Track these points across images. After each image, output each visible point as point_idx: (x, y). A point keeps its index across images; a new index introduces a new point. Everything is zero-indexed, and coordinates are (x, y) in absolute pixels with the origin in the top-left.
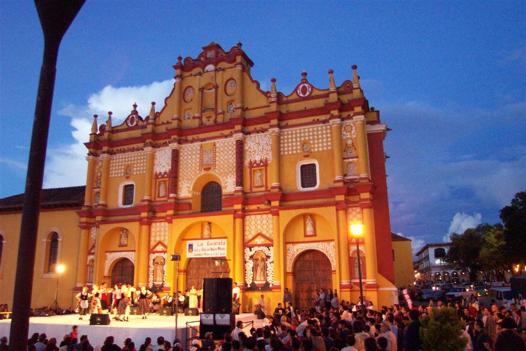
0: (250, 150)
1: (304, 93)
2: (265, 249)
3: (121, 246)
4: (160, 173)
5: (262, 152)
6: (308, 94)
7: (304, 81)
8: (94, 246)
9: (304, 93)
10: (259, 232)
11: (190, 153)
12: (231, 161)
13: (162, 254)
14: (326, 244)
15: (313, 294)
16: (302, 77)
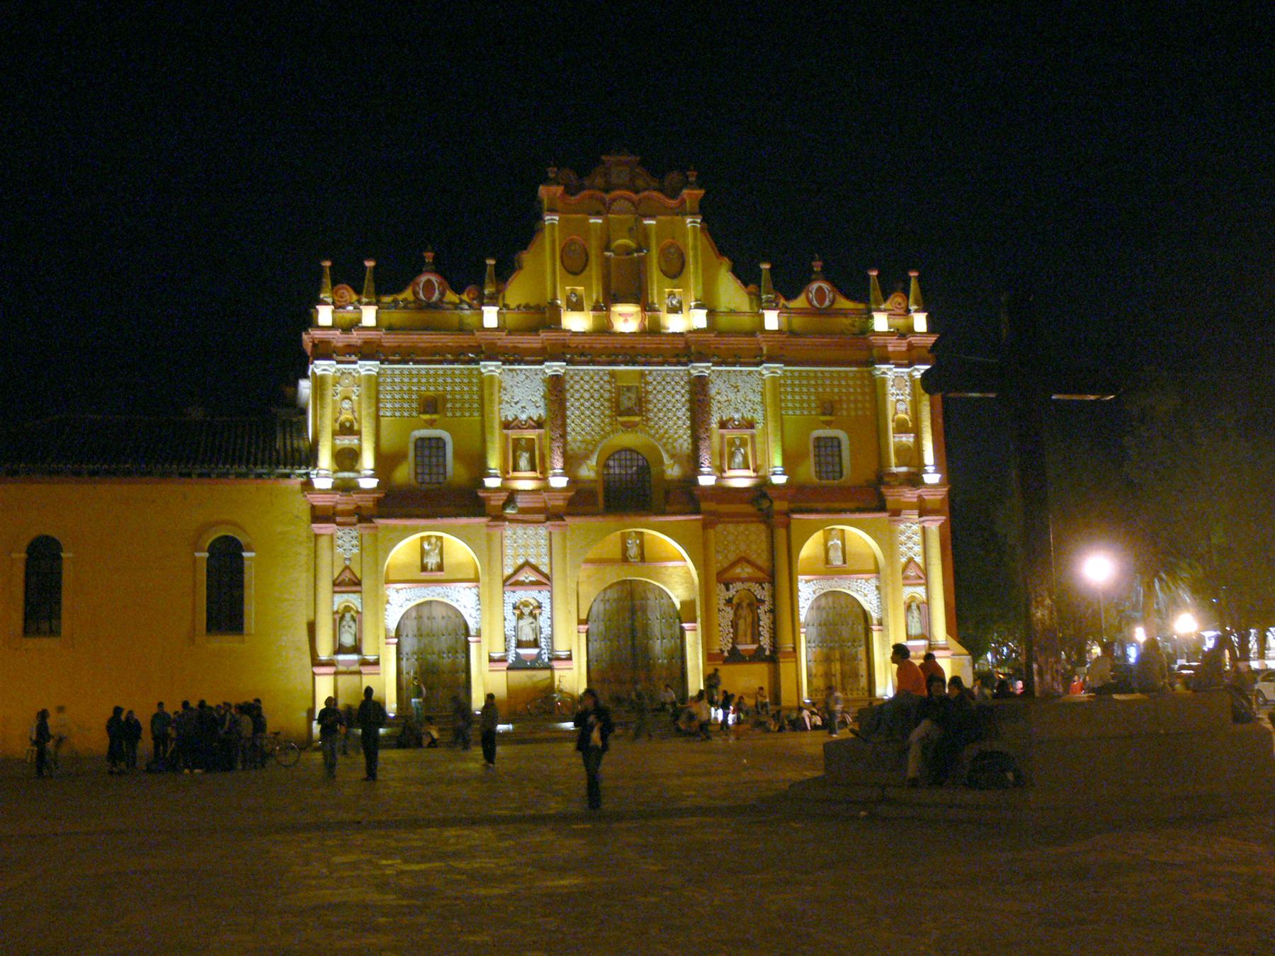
0: (718, 397)
1: (821, 301)
2: (756, 588)
5: (744, 404)
6: (827, 303)
9: (821, 301)
11: (587, 387)
12: (680, 414)
15: (833, 667)
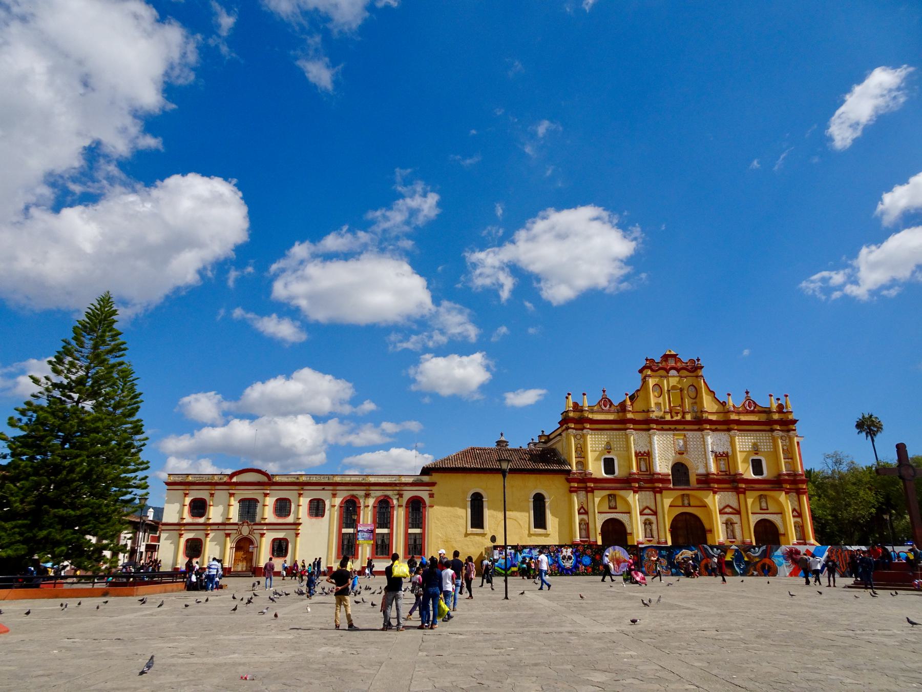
3: (610, 508)
4: (640, 452)
6: (752, 408)
7: (748, 398)
8: (582, 507)
10: (727, 504)
13: (650, 517)
14: (775, 515)
16: (746, 395)
